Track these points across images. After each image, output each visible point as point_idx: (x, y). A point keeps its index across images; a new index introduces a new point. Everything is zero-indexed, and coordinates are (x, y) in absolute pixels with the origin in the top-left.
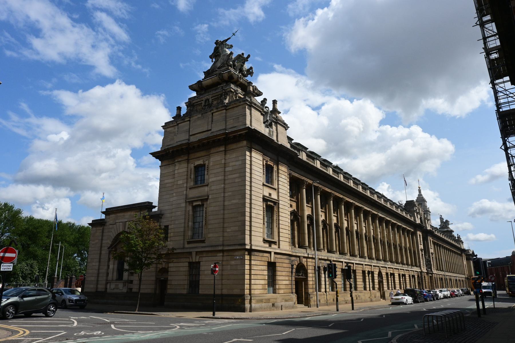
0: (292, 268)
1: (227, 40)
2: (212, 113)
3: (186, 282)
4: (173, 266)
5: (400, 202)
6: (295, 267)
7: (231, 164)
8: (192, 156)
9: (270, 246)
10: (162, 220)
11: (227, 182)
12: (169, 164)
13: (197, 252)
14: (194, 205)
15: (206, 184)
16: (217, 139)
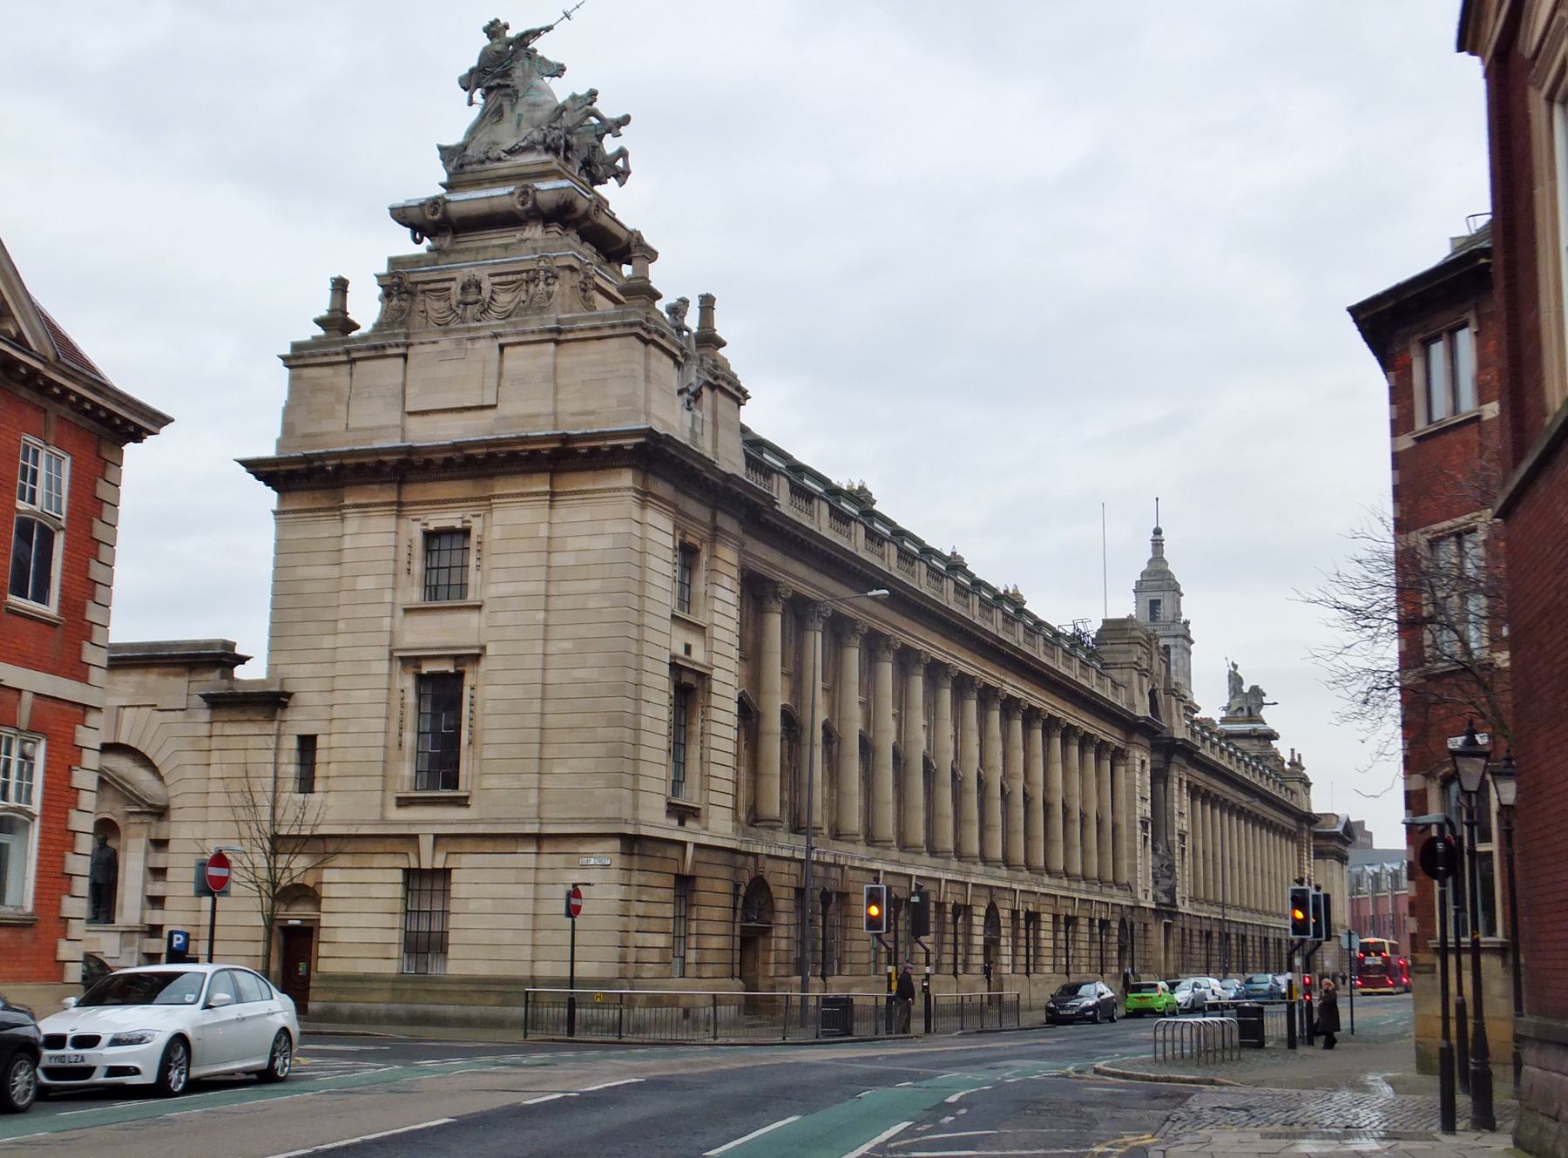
0: (736, 895)
1: (536, 34)
2: (502, 347)
3: (396, 936)
4: (337, 881)
5: (1080, 626)
6: (743, 890)
7: (573, 543)
8: (413, 492)
9: (682, 823)
10: (289, 715)
11: (556, 603)
12: (319, 510)
13: (437, 837)
14: (424, 671)
15: (472, 598)
16: (525, 451)
